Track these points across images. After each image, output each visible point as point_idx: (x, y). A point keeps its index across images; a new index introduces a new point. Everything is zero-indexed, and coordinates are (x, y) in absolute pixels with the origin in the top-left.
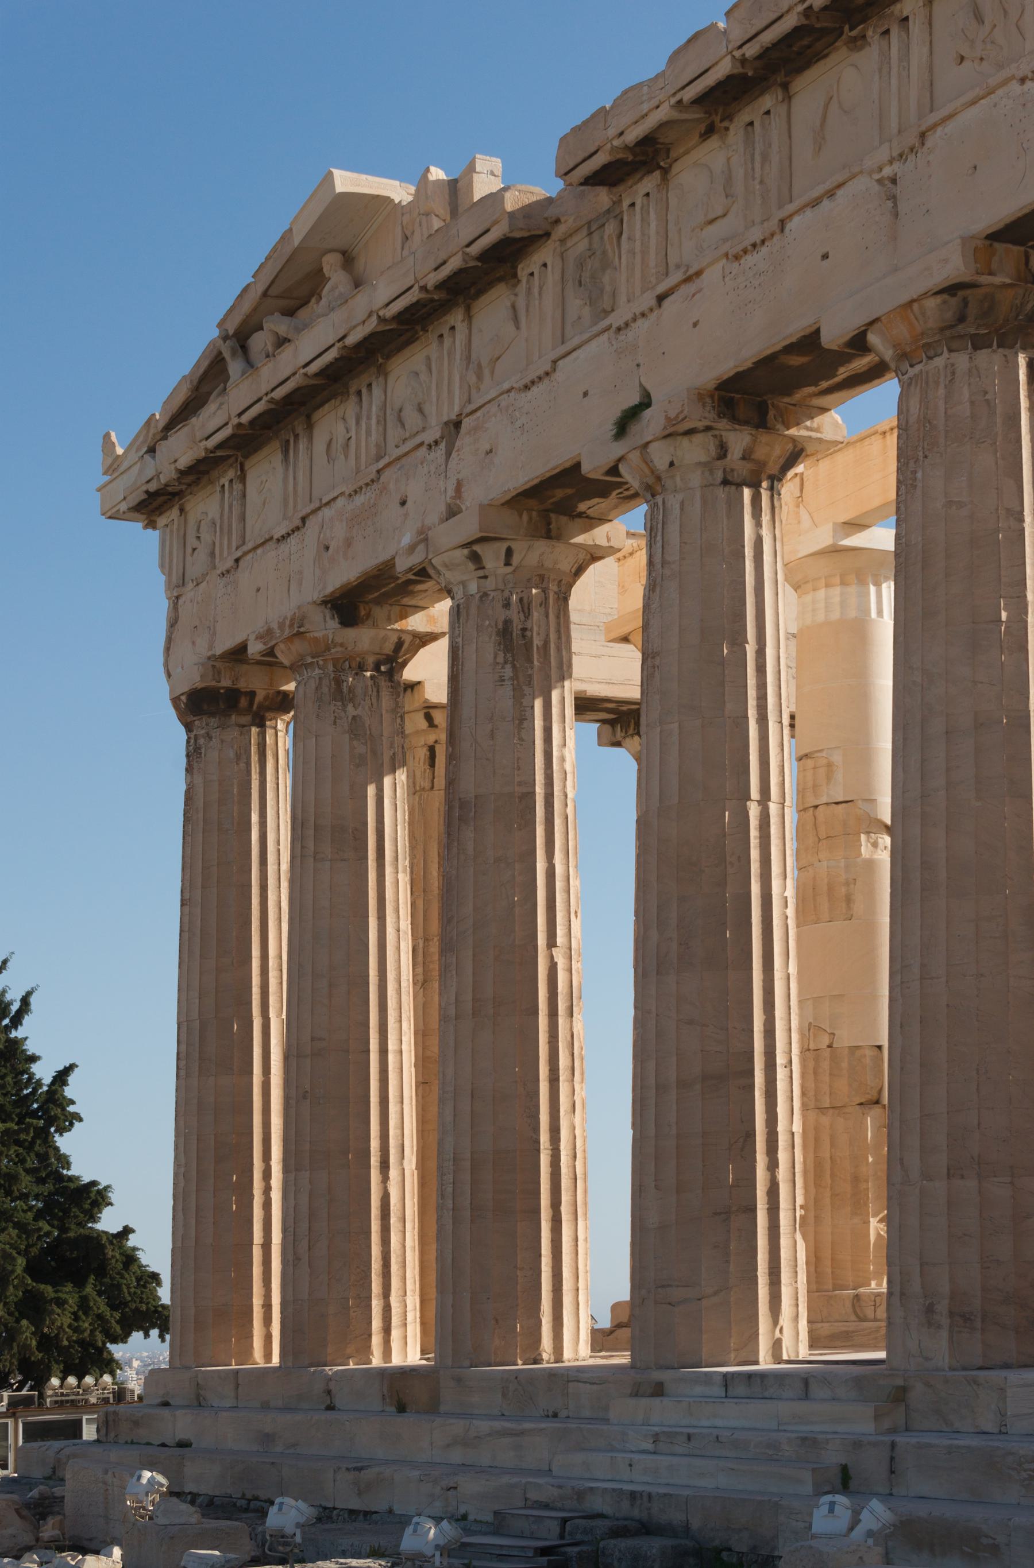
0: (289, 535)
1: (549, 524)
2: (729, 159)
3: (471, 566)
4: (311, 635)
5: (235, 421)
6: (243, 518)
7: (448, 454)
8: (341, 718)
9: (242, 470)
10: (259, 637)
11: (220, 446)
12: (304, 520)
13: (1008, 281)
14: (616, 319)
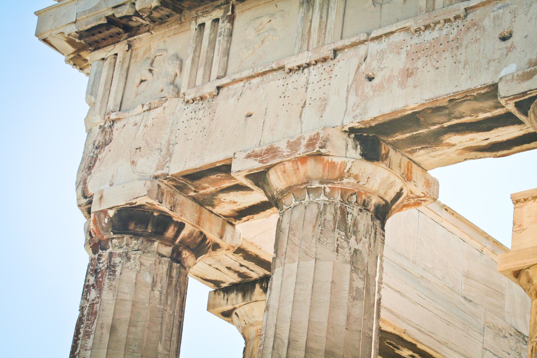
0: (309, 65)
4: (330, 159)
6: (227, 53)
8: (343, 248)
12: (335, 52)
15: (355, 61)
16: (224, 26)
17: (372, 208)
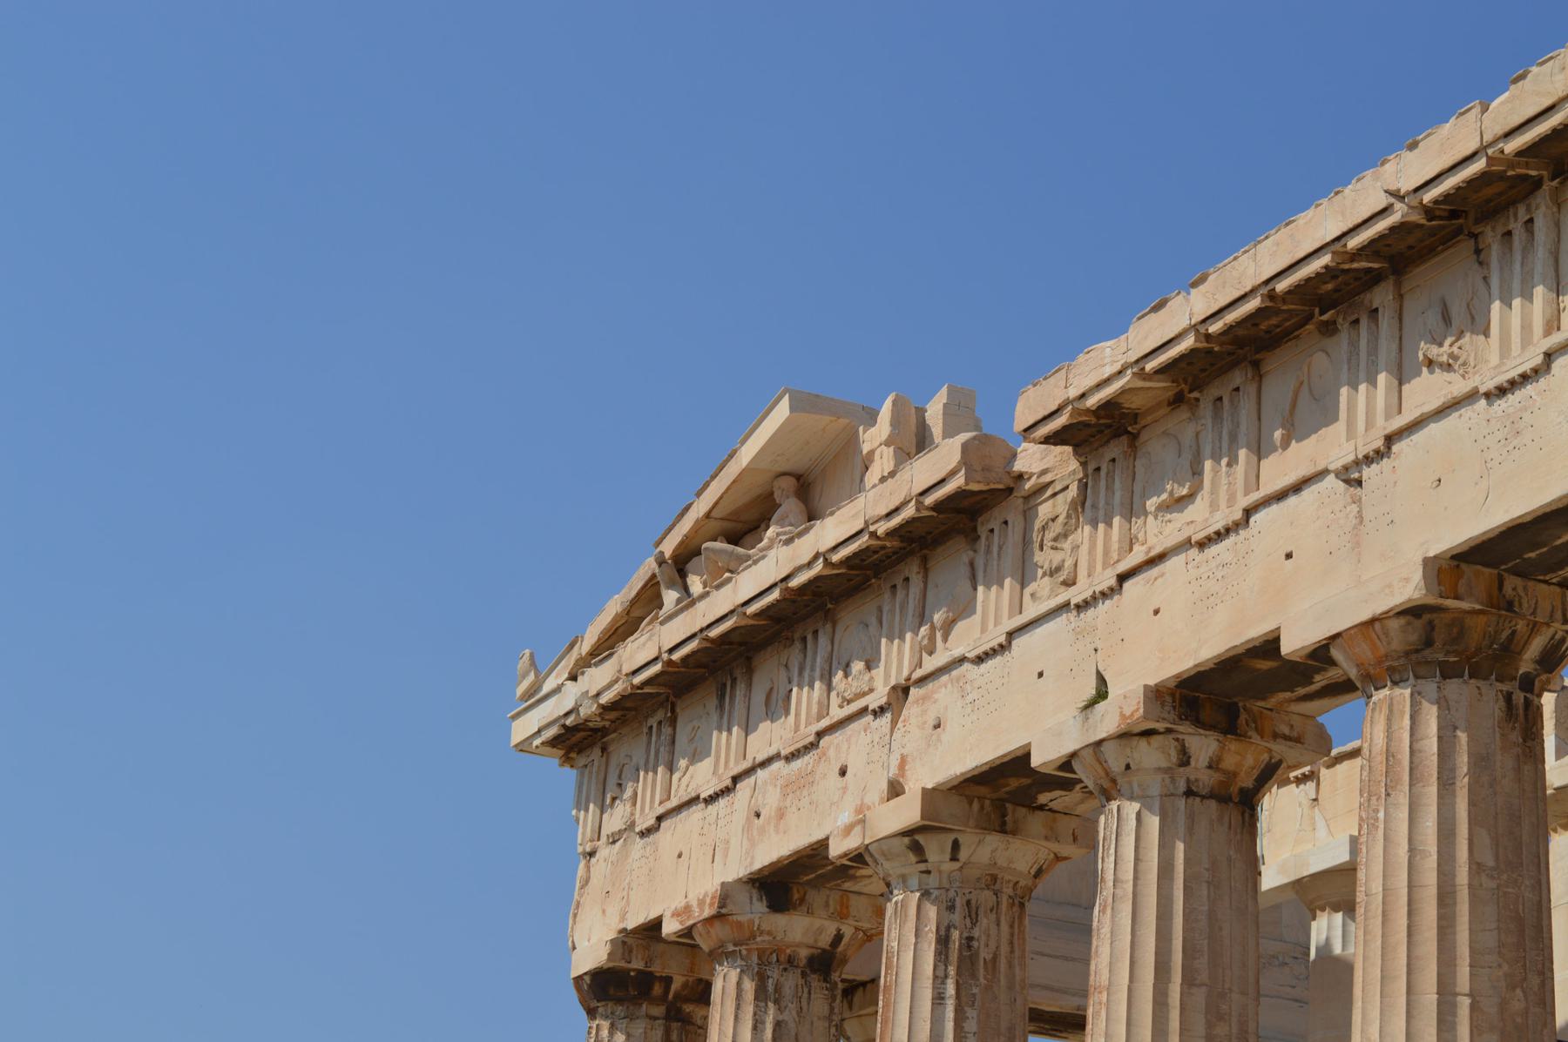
1: (1004, 815)
2: (1197, 434)
3: (912, 858)
5: (665, 656)
7: (894, 723)
9: (673, 711)
10: (676, 914)
11: (649, 682)
13: (1478, 607)
14: (1076, 595)
15: (748, 792)
16: (667, 730)
17: (803, 962)
